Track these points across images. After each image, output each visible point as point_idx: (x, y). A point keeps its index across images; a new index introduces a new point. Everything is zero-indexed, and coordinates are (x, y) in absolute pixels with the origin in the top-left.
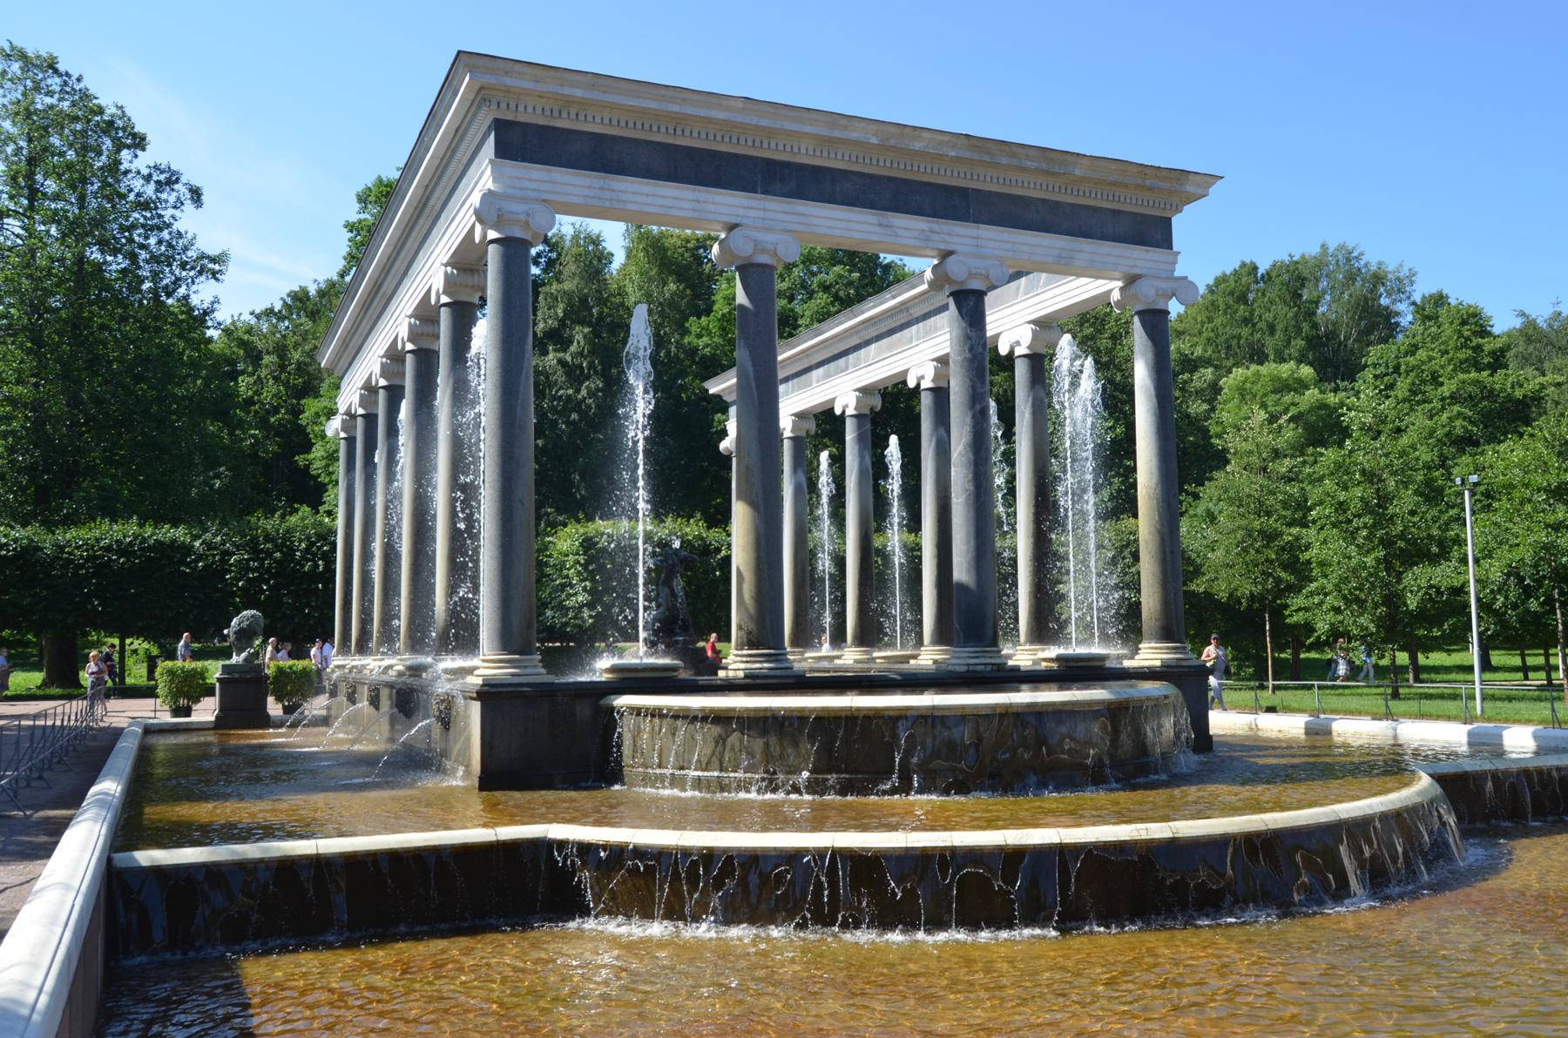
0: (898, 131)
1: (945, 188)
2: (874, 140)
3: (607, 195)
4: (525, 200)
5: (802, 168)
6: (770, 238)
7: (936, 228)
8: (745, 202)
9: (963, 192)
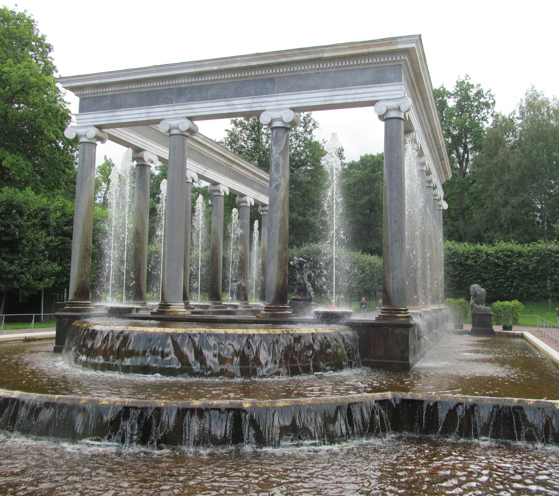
0: (224, 61)
1: (263, 80)
2: (215, 68)
3: (115, 118)
4: (86, 127)
5: (193, 88)
6: (174, 123)
7: (255, 100)
8: (167, 109)
9: (271, 80)
